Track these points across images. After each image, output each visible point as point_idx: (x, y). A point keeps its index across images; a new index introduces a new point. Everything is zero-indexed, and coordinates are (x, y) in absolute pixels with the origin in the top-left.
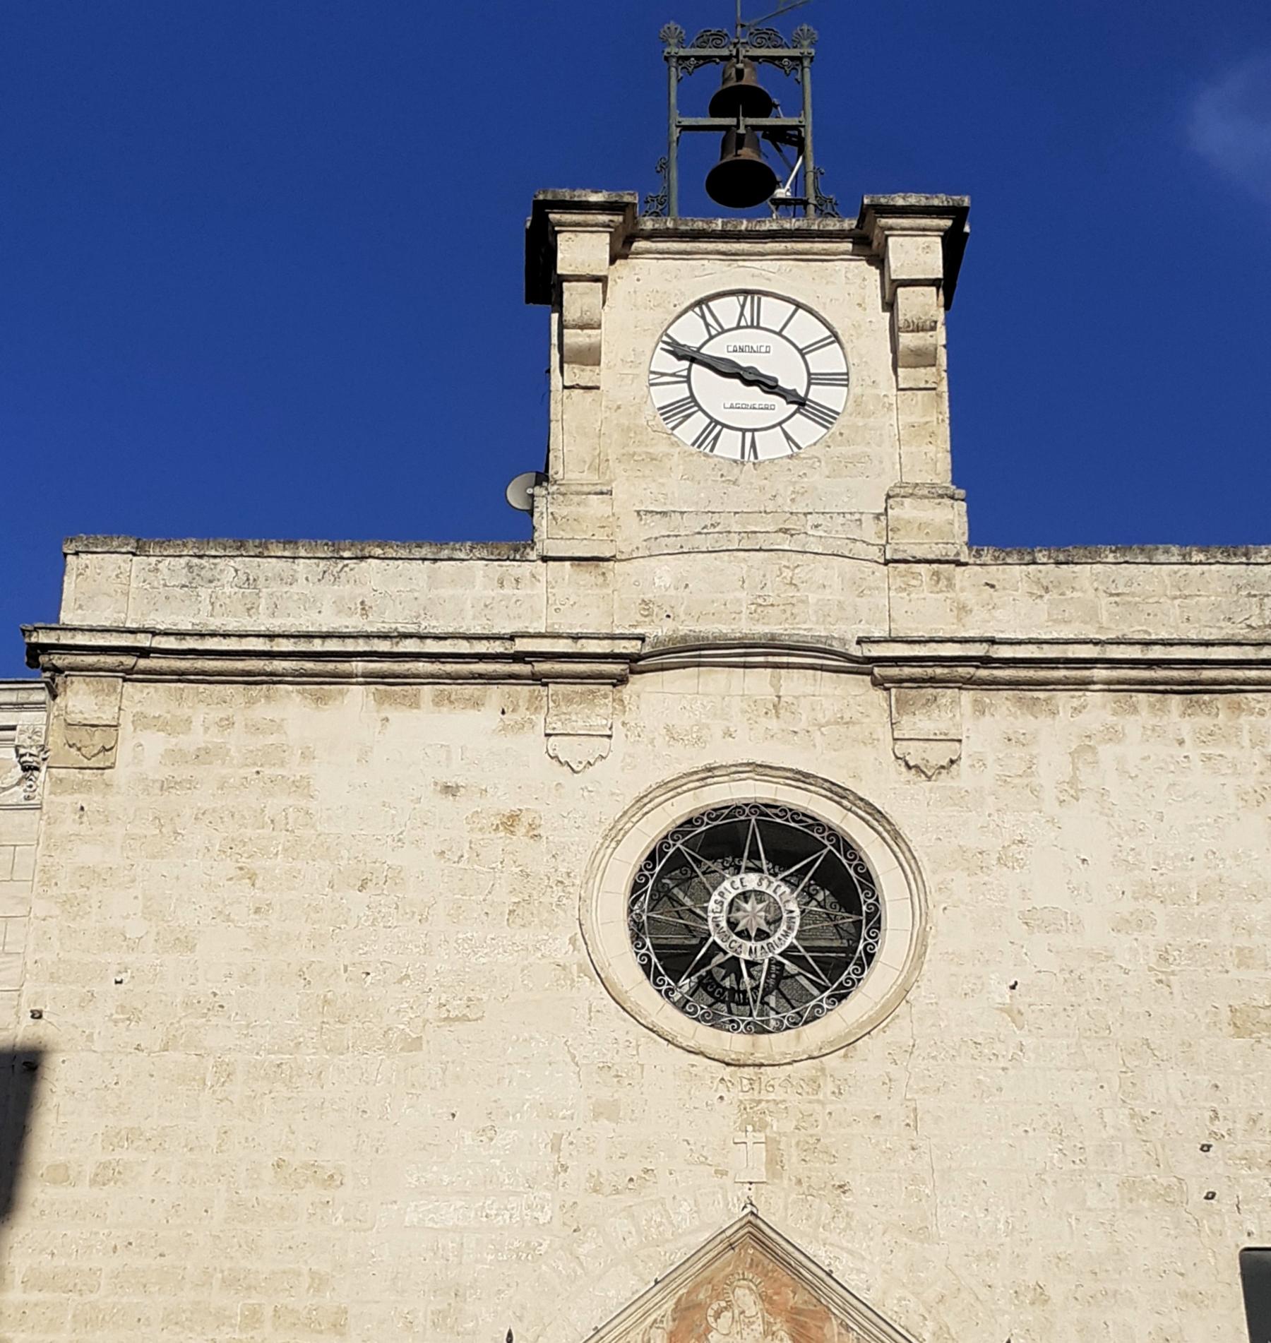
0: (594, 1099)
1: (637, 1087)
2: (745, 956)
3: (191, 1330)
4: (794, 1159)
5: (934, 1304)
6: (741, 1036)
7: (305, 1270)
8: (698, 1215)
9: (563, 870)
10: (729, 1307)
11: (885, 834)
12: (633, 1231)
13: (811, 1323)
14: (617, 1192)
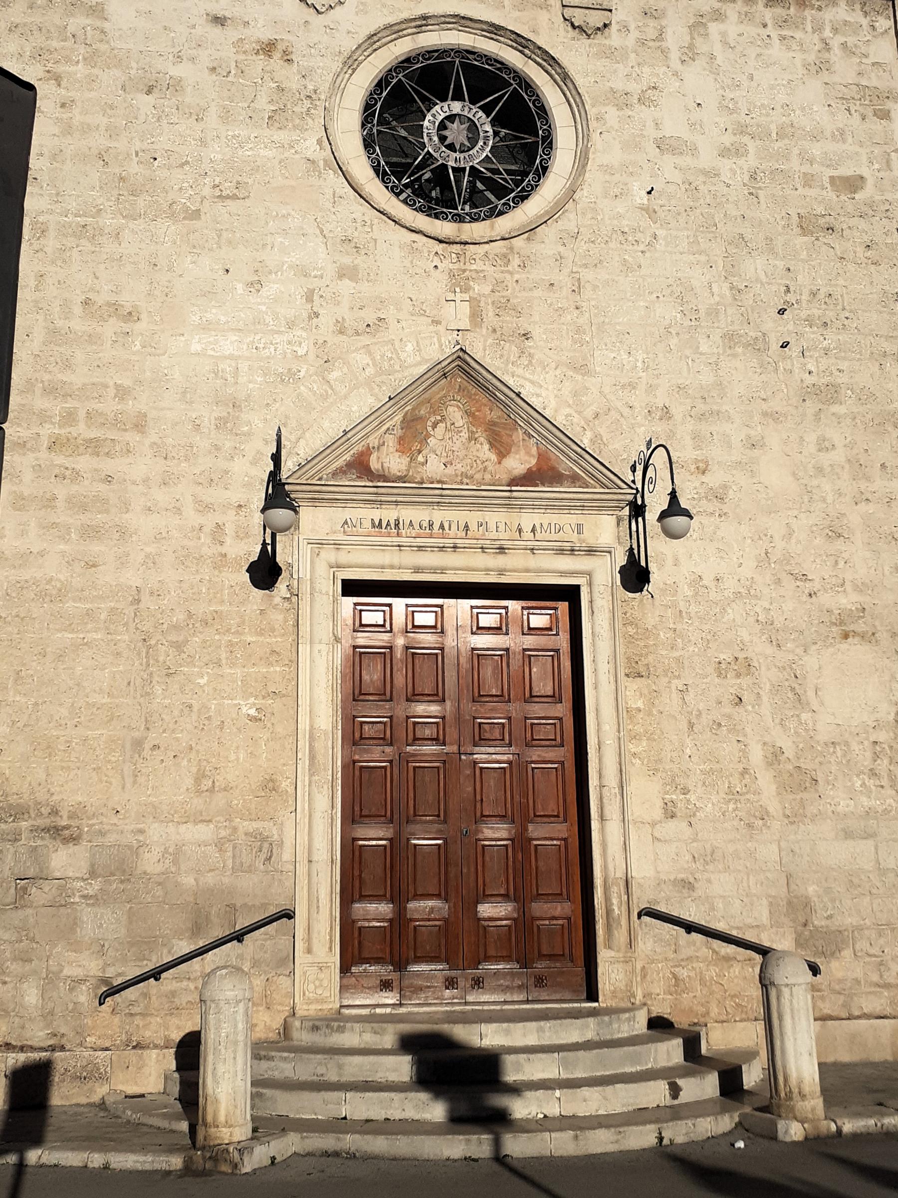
0: (338, 263)
1: (371, 256)
2: (451, 163)
3: (19, 425)
4: (491, 314)
5: (591, 419)
6: (450, 224)
7: (111, 384)
8: (419, 350)
9: (311, 87)
10: (443, 419)
11: (557, 77)
12: (370, 363)
13: (503, 432)
14: (357, 334)
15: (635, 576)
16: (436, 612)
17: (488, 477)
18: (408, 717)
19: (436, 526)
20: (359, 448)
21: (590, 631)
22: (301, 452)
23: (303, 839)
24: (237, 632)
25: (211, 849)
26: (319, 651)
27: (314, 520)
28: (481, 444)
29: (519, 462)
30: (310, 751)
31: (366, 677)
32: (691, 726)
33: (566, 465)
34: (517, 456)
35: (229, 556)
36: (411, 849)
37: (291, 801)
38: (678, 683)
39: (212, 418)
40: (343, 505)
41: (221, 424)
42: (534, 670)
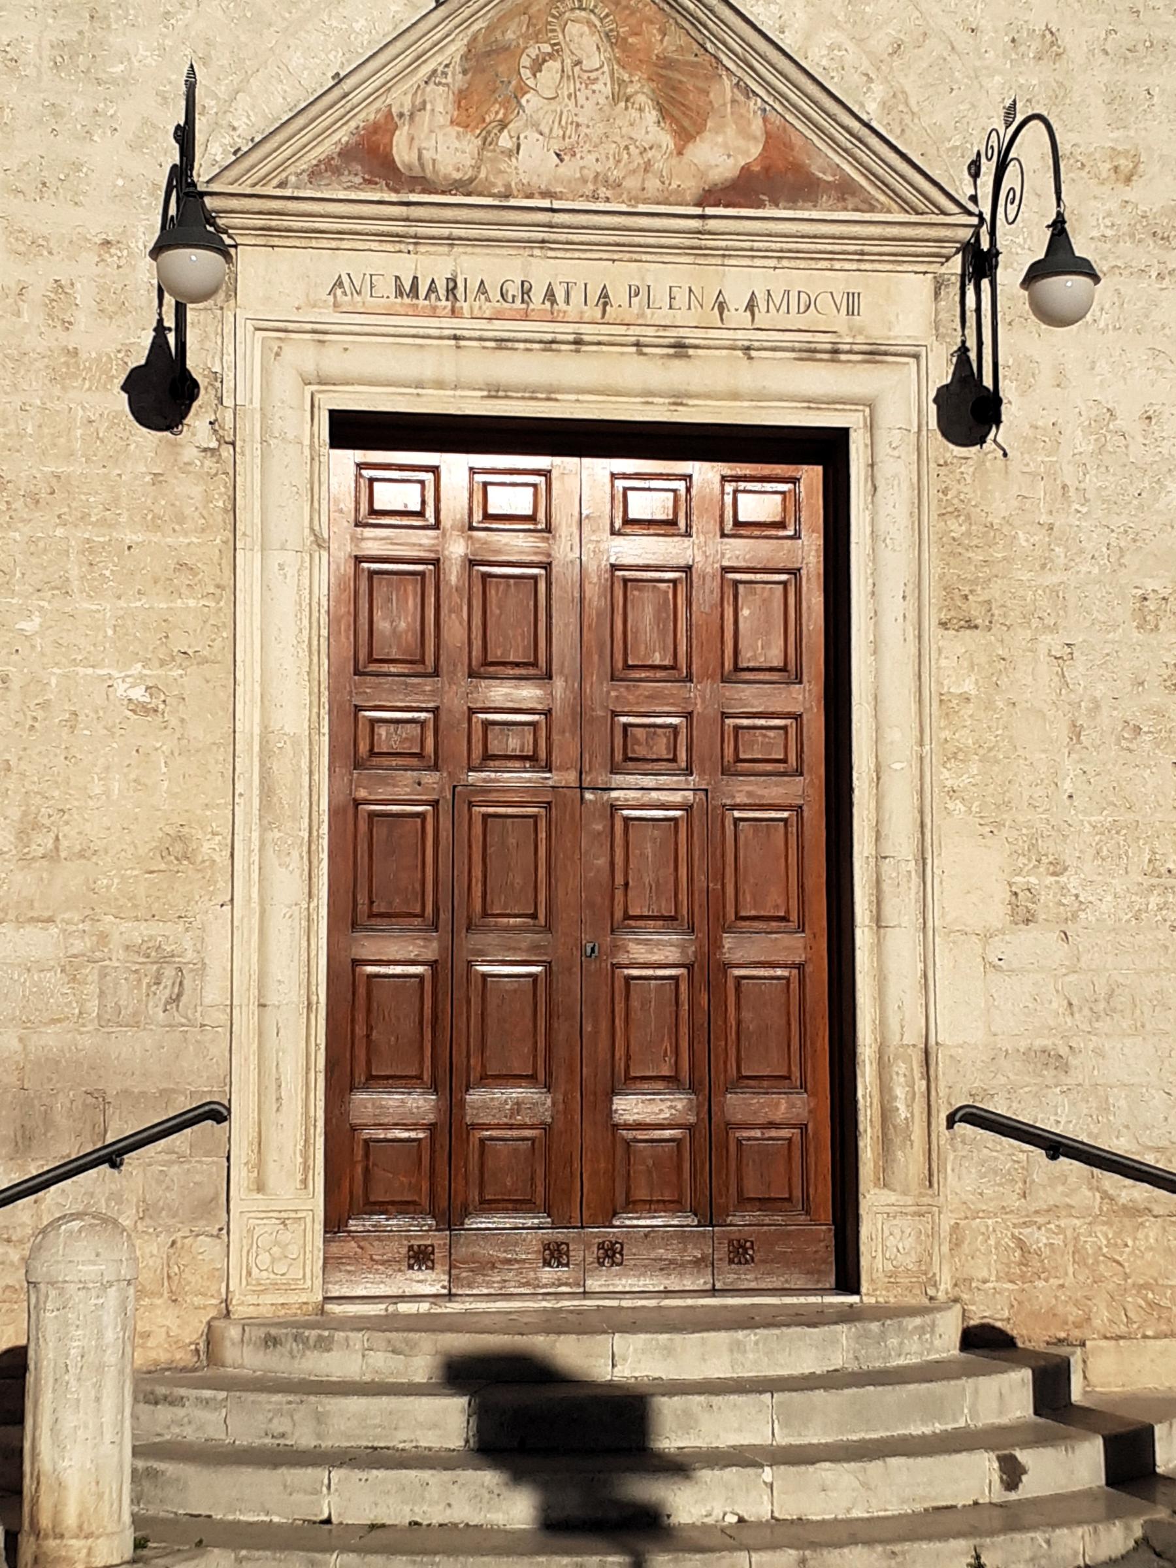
10: (556, 52)
15: (970, 409)
16: (535, 486)
17: (653, 184)
18: (472, 711)
19: (538, 295)
20: (370, 114)
21: (868, 530)
22: (241, 123)
23: (246, 961)
24: (103, 522)
25: (53, 978)
26: (281, 567)
27: (270, 278)
28: (641, 110)
29: (723, 153)
30: (263, 779)
31: (382, 625)
32: (1076, 731)
33: (826, 160)
34: (720, 139)
35: (83, 355)
36: (476, 984)
37: (222, 883)
38: (1052, 642)
39: (46, 44)
40: (334, 244)
41: (64, 56)
42: (745, 612)
